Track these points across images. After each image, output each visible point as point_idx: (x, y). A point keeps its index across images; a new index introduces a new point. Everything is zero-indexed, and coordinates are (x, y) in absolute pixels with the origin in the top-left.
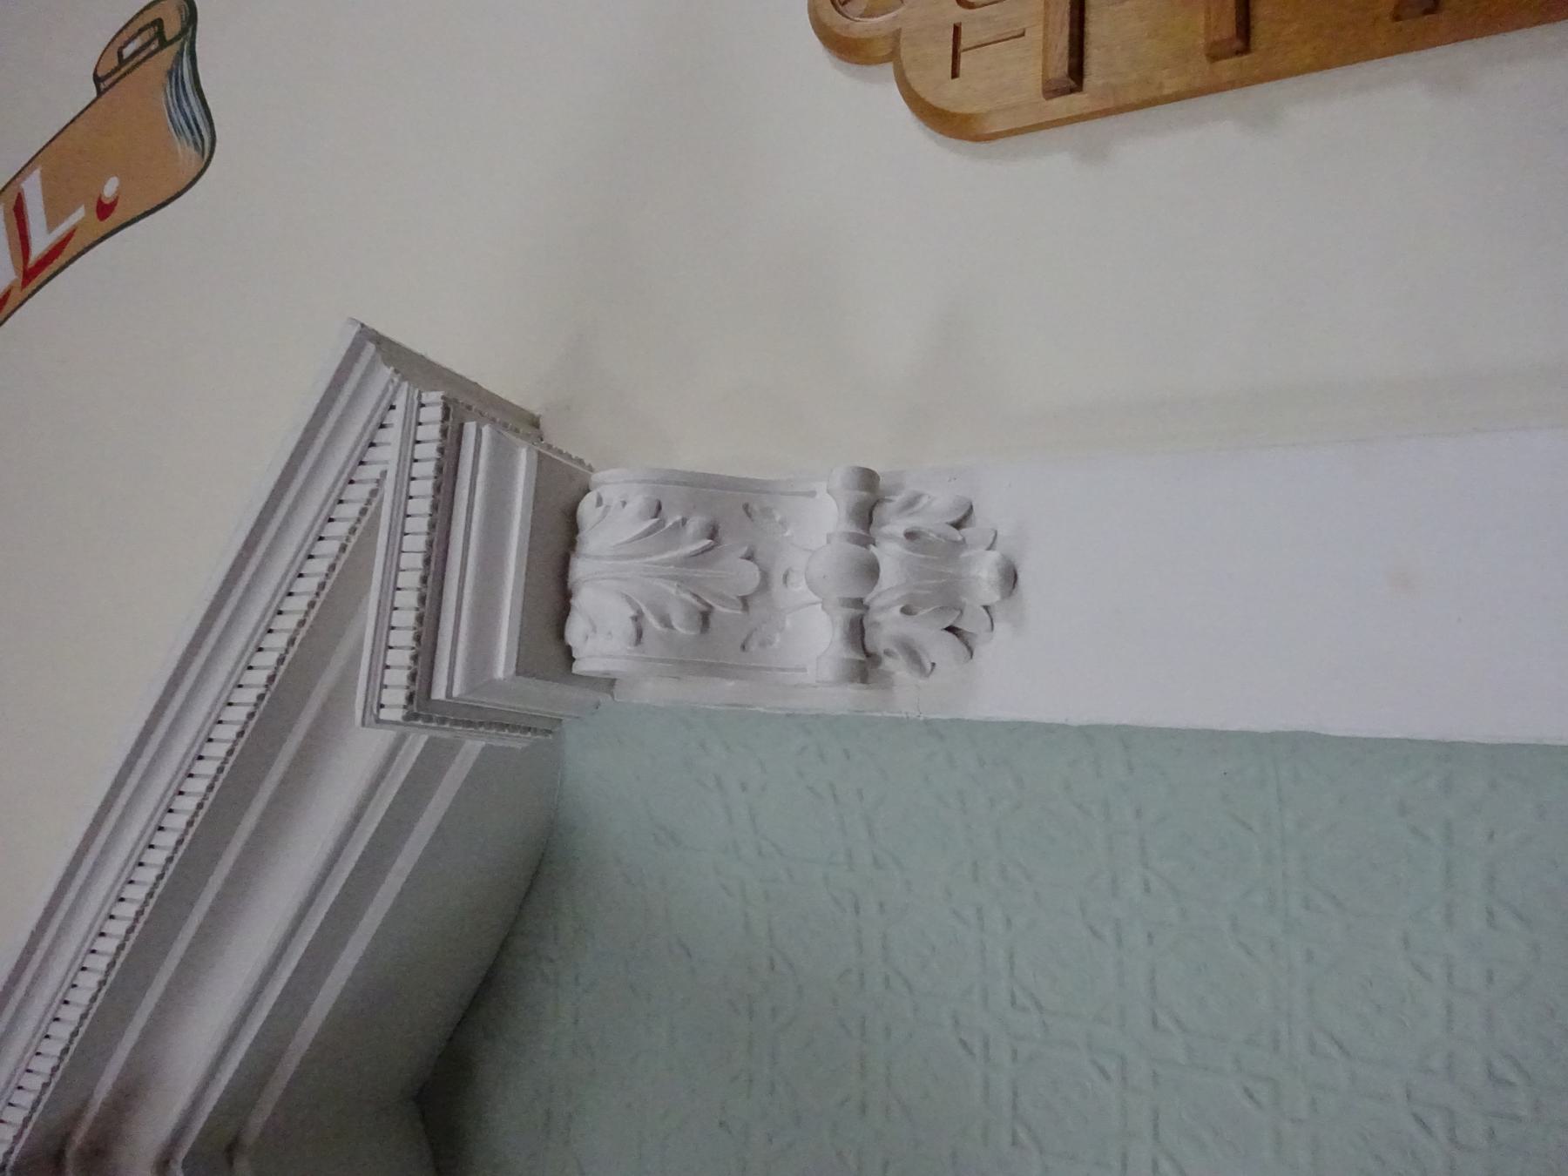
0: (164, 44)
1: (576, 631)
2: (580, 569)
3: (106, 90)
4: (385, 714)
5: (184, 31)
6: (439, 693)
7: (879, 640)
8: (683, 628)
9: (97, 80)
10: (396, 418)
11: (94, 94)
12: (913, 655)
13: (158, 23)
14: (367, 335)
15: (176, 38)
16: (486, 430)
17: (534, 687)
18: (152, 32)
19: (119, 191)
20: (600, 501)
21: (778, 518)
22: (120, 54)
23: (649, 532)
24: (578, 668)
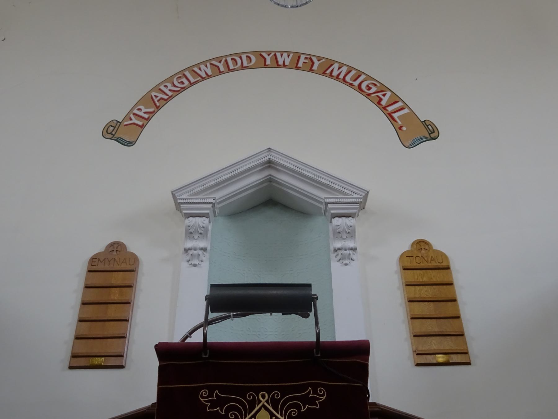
0: (430, 134)
1: (337, 219)
2: (344, 218)
3: (423, 123)
4: (326, 199)
5: (431, 138)
6: (329, 205)
7: (338, 252)
8: (338, 231)
9: (424, 121)
10: (359, 196)
11: (422, 121)
13: (434, 132)
14: (368, 192)
15: (430, 136)
16: (358, 206)
17: (330, 214)
18: (432, 131)
19: (403, 130)
20: (351, 220)
21: (351, 240)
22: (429, 125)
23: (348, 226)
24: (332, 219)
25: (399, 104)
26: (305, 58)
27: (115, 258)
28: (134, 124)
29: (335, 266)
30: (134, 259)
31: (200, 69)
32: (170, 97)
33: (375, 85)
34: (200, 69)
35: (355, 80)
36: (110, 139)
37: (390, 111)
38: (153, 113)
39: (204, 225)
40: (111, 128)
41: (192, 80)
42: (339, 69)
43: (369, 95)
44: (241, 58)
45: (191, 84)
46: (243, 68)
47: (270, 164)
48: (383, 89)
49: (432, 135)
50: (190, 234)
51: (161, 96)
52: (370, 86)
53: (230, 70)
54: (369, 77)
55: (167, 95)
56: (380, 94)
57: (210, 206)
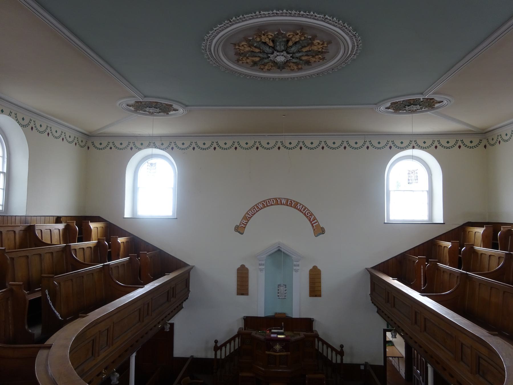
25: (316, 221)
26: (290, 201)
28: (242, 226)
29: (294, 273)
30: (247, 270)
33: (310, 213)
35: (304, 211)
38: (247, 223)
40: (236, 228)
41: (257, 210)
42: (300, 206)
43: (307, 217)
44: (271, 201)
45: (257, 211)
46: (272, 205)
48: (312, 215)
49: (323, 233)
50: (260, 265)
53: (268, 206)
54: (308, 210)
55: (250, 216)
56: (310, 217)
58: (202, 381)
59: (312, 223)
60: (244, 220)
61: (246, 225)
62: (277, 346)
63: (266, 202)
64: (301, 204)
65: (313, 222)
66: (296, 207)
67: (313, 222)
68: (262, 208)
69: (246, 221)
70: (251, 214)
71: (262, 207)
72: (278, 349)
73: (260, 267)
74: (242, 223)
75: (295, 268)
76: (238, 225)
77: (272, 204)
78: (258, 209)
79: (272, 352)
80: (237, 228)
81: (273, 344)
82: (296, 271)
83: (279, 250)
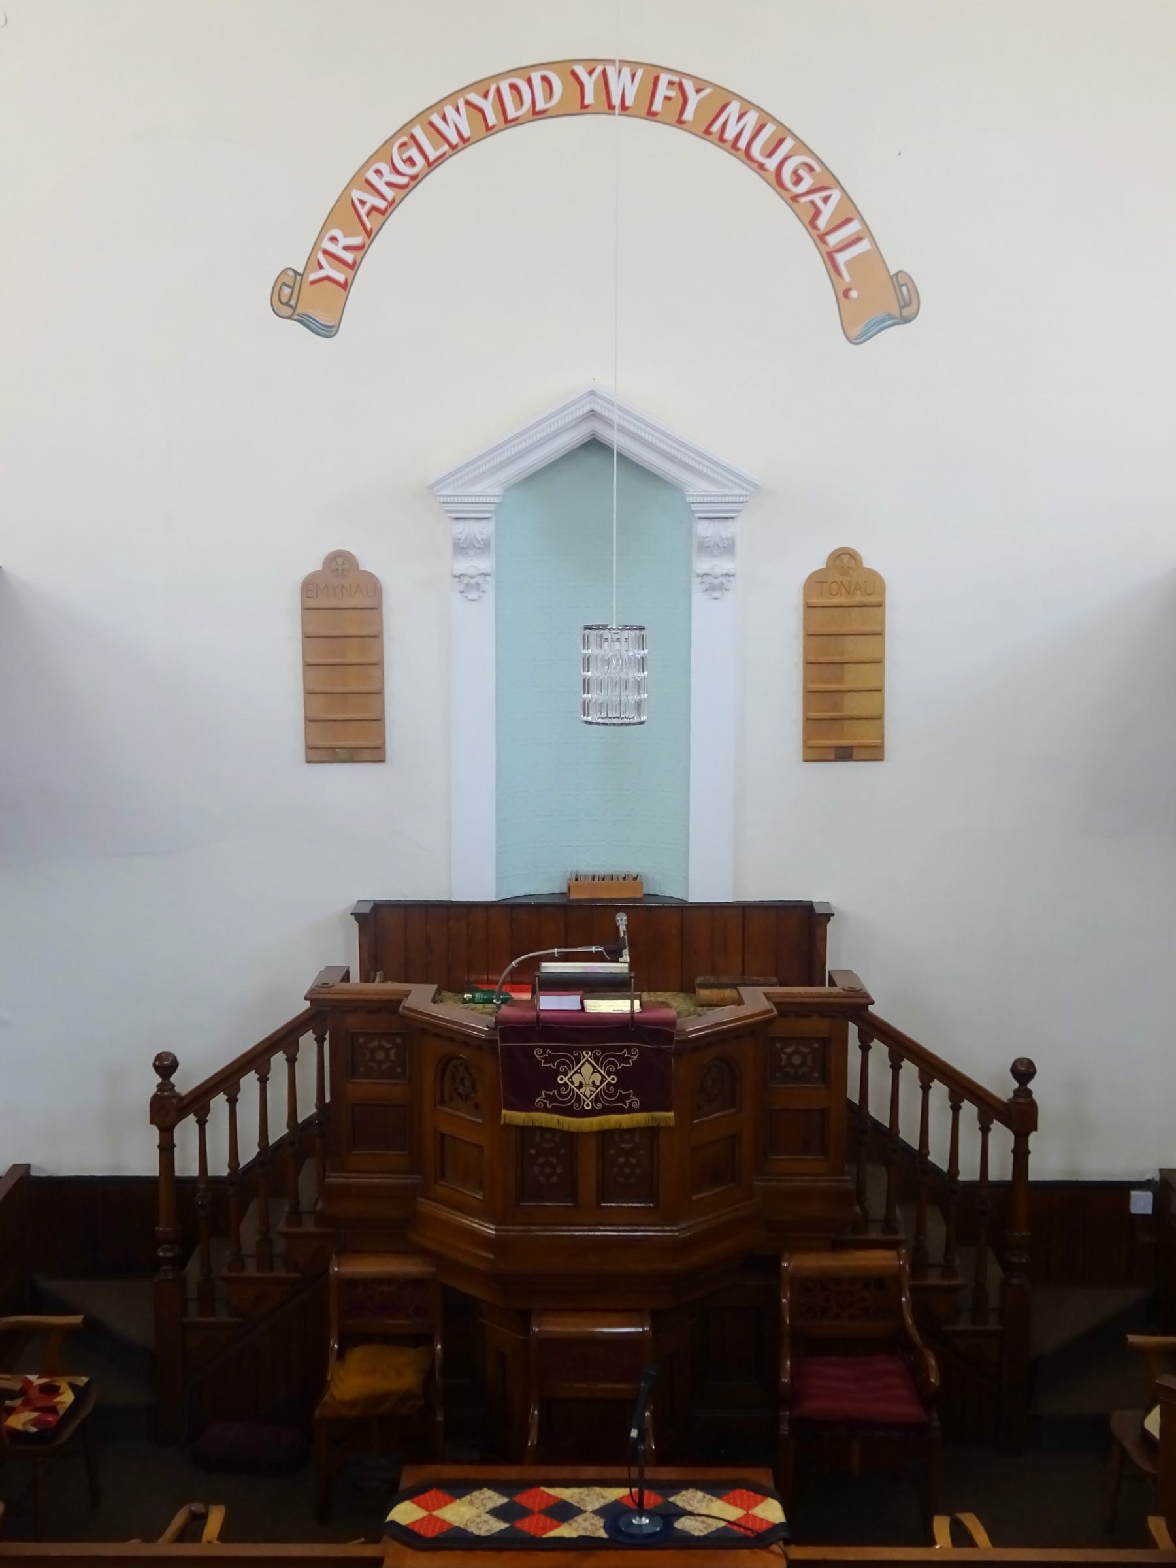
0: (901, 308)
7: (705, 578)
12: (702, 583)
22: (905, 284)
25: (853, 228)
26: (671, 83)
27: (342, 585)
28: (328, 278)
29: (699, 599)
30: (372, 586)
31: (444, 118)
32: (391, 203)
33: (811, 169)
34: (444, 118)
35: (770, 155)
36: (289, 318)
37: (834, 246)
39: (484, 537)
40: (287, 291)
41: (432, 155)
42: (740, 117)
43: (795, 198)
44: (529, 82)
45: (431, 165)
46: (537, 114)
47: (593, 414)
48: (826, 183)
49: (906, 312)
50: (461, 548)
51: (373, 200)
52: (801, 172)
53: (509, 122)
54: (801, 147)
55: (384, 198)
56: (817, 198)
57: (492, 507)
58: (78, 1319)
59: (824, 242)
60: (336, 232)
61: (353, 266)
62: (579, 1072)
63: (498, 91)
64: (747, 106)
65: (833, 240)
66: (716, 128)
67: (833, 240)
68: (465, 141)
69: (357, 241)
70: (389, 184)
71: (466, 133)
72: (587, 1090)
73: (464, 565)
74: (326, 252)
75: (703, 565)
76: (301, 271)
77: (539, 107)
78: (436, 148)
79: (545, 1110)
80: (292, 288)
81: (547, 1060)
82: (712, 588)
83: (595, 445)
